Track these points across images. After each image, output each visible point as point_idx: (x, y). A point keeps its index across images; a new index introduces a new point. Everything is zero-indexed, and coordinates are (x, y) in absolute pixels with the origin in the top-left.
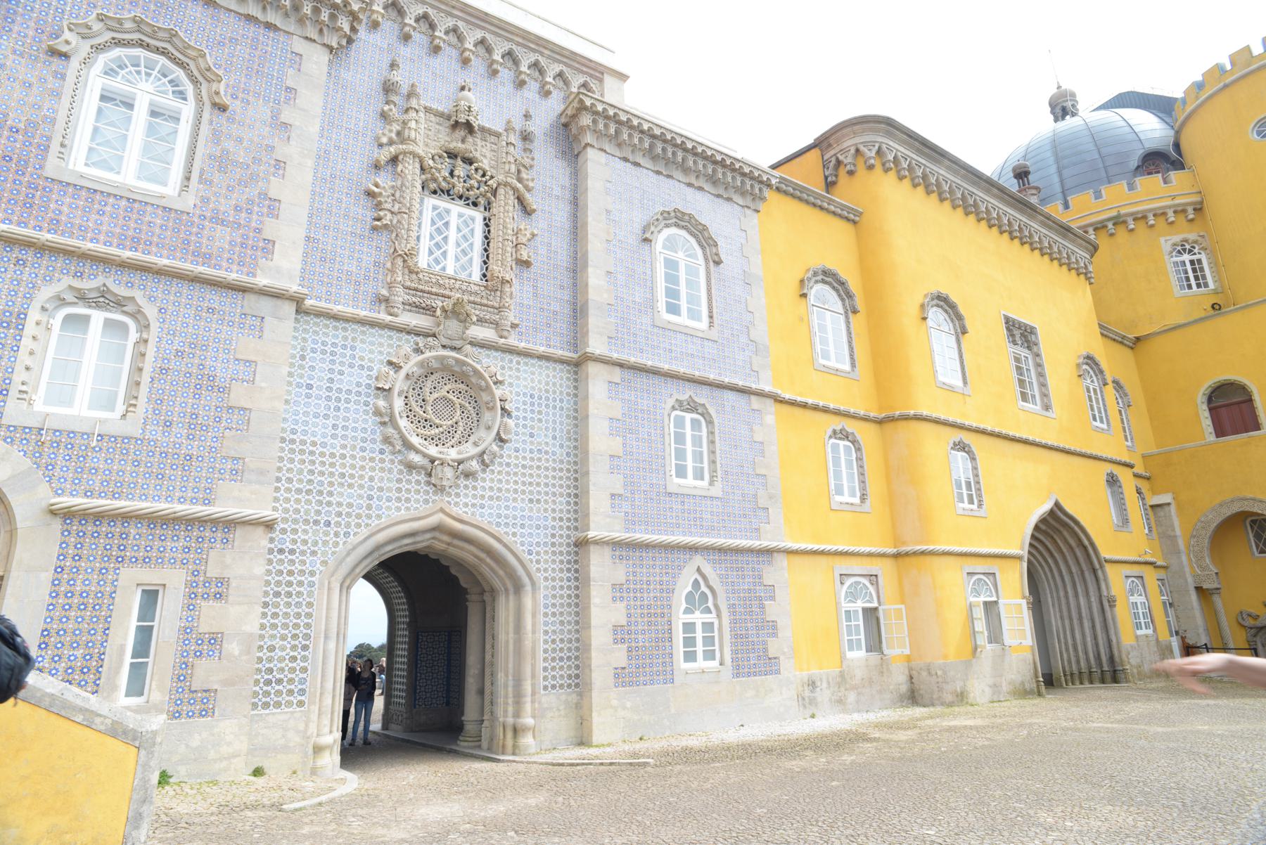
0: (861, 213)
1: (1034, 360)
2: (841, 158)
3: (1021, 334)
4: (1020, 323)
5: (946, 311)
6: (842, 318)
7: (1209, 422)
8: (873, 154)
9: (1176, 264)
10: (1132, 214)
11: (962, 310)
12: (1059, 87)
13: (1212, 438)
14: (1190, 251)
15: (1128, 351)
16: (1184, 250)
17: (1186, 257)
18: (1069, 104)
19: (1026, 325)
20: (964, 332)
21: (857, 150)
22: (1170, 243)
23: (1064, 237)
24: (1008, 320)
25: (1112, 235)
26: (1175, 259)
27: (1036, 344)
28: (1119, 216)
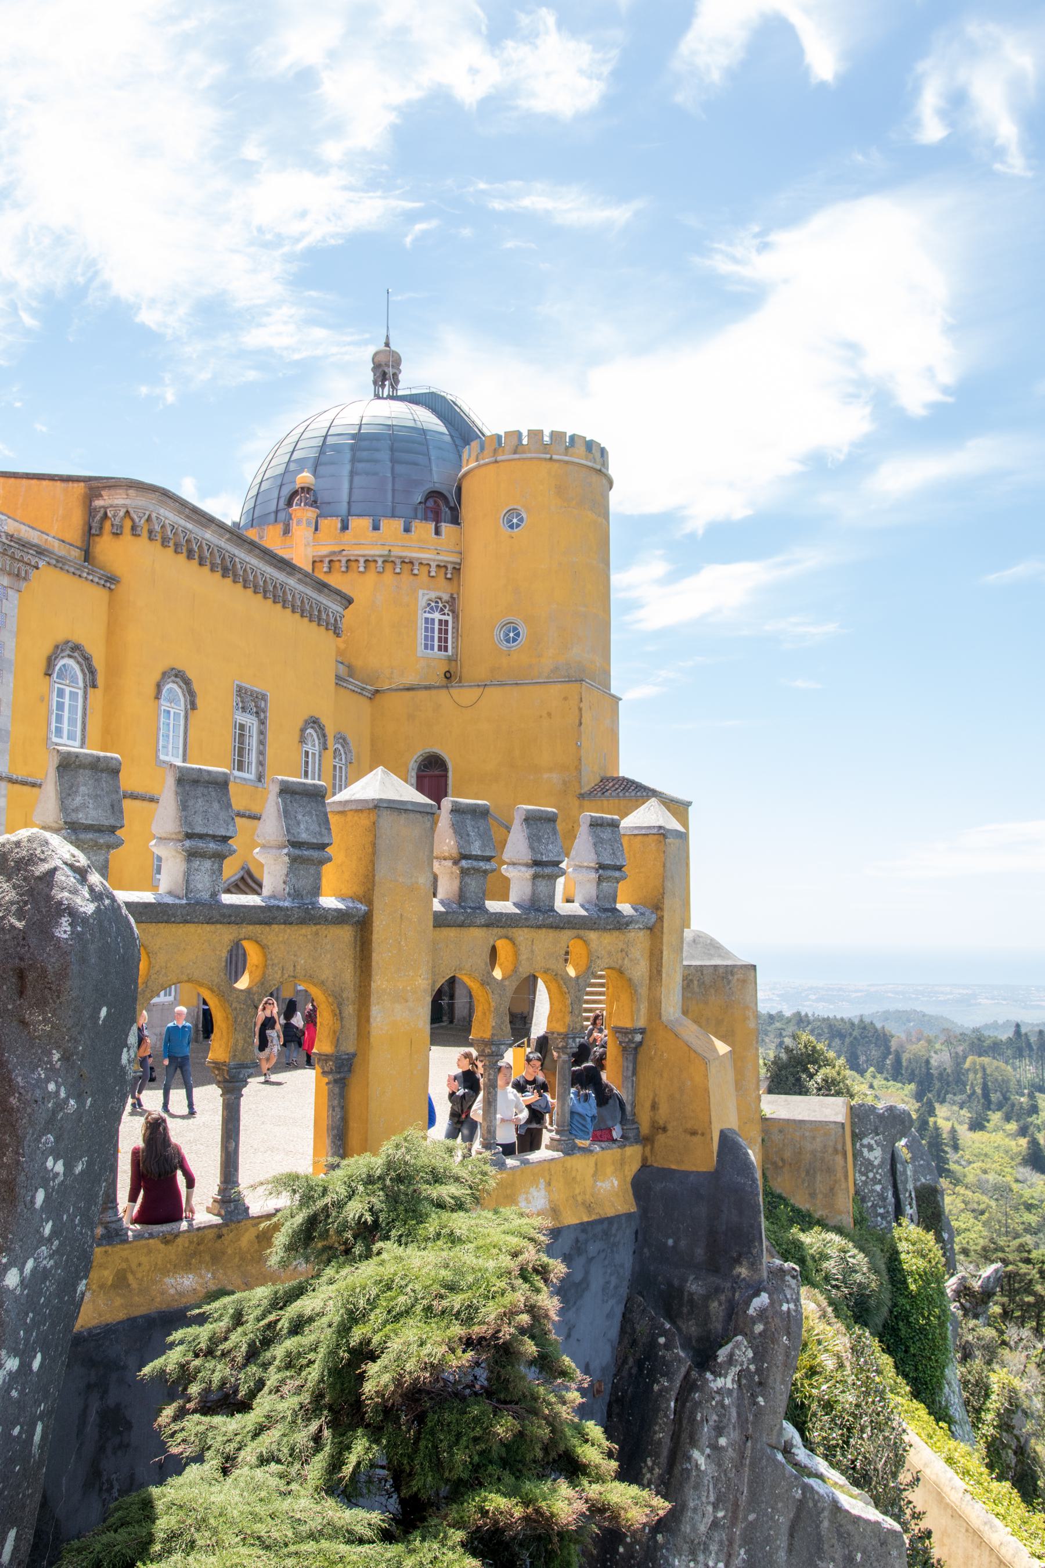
0: (118, 582)
1: (259, 727)
2: (109, 515)
6: (80, 693)
8: (143, 521)
9: (427, 619)
10: (401, 557)
11: (195, 686)
12: (387, 345)
15: (363, 702)
16: (437, 607)
17: (437, 616)
18: (390, 371)
19: (257, 693)
20: (193, 706)
21: (127, 512)
22: (426, 597)
23: (320, 591)
26: (430, 616)
28: (389, 556)
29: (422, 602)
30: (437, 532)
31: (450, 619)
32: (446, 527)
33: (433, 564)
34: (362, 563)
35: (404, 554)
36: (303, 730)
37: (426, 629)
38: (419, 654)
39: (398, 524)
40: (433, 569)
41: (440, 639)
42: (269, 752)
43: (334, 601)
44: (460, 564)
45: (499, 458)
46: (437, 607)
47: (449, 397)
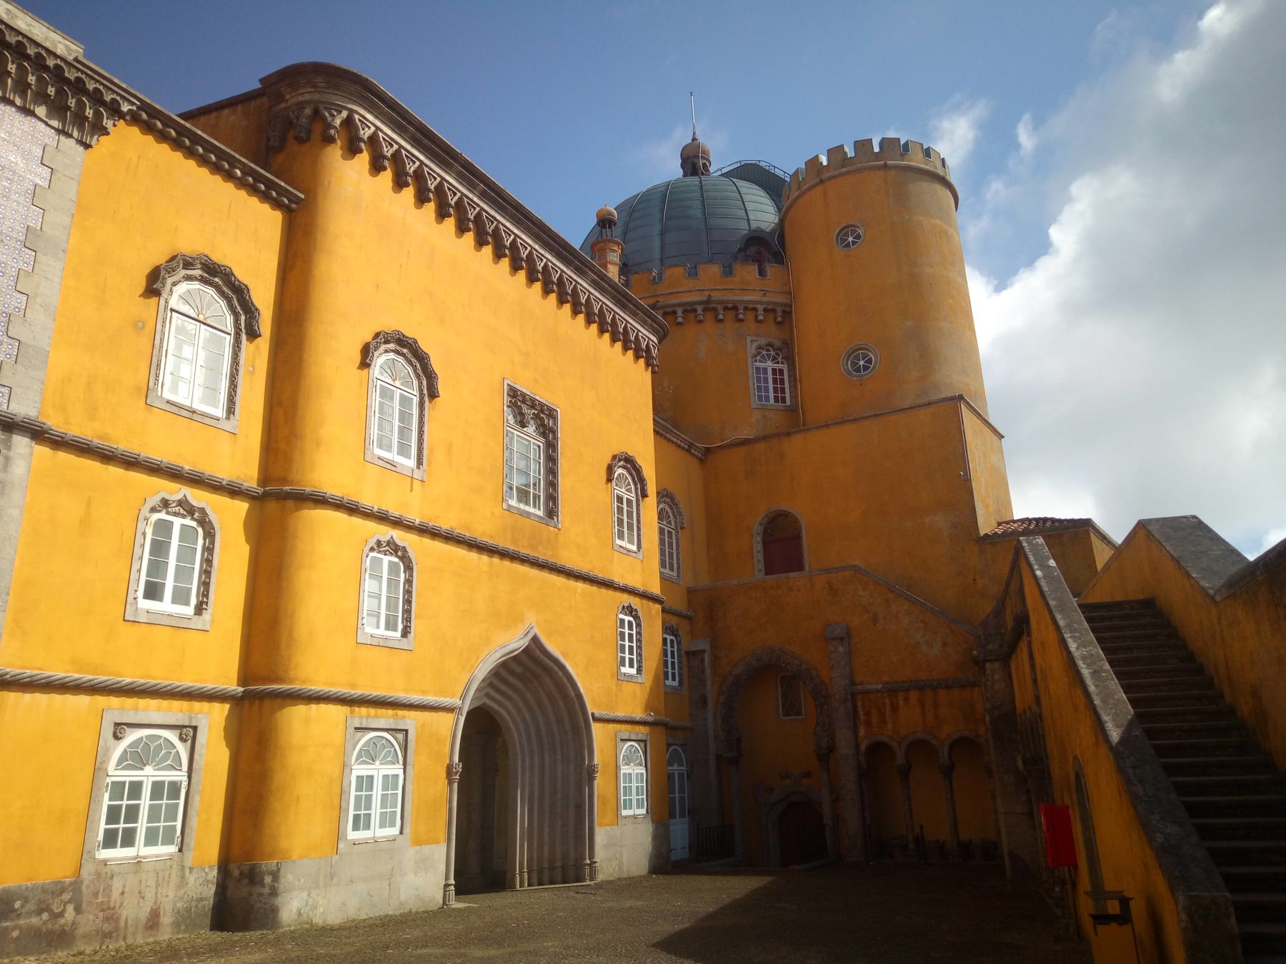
3: (531, 412)
4: (533, 400)
5: (410, 363)
7: (760, 557)
9: (758, 369)
10: (722, 302)
11: (436, 364)
13: (759, 575)
14: (774, 359)
16: (769, 356)
17: (769, 365)
19: (542, 405)
20: (433, 395)
22: (755, 345)
24: (513, 393)
25: (700, 321)
26: (758, 364)
27: (554, 432)
28: (709, 301)
29: (751, 349)
30: (762, 273)
31: (785, 368)
32: (771, 269)
33: (760, 308)
34: (680, 313)
35: (726, 298)
36: (610, 470)
37: (759, 380)
38: (753, 406)
39: (715, 269)
40: (761, 311)
41: (775, 390)
42: (563, 482)
43: (643, 323)
44: (791, 306)
45: (824, 177)
46: (769, 356)
47: (762, 164)
